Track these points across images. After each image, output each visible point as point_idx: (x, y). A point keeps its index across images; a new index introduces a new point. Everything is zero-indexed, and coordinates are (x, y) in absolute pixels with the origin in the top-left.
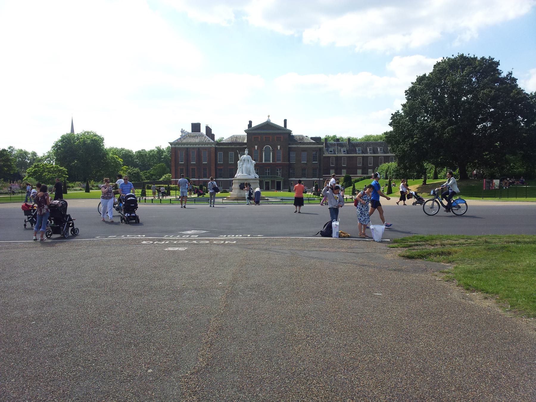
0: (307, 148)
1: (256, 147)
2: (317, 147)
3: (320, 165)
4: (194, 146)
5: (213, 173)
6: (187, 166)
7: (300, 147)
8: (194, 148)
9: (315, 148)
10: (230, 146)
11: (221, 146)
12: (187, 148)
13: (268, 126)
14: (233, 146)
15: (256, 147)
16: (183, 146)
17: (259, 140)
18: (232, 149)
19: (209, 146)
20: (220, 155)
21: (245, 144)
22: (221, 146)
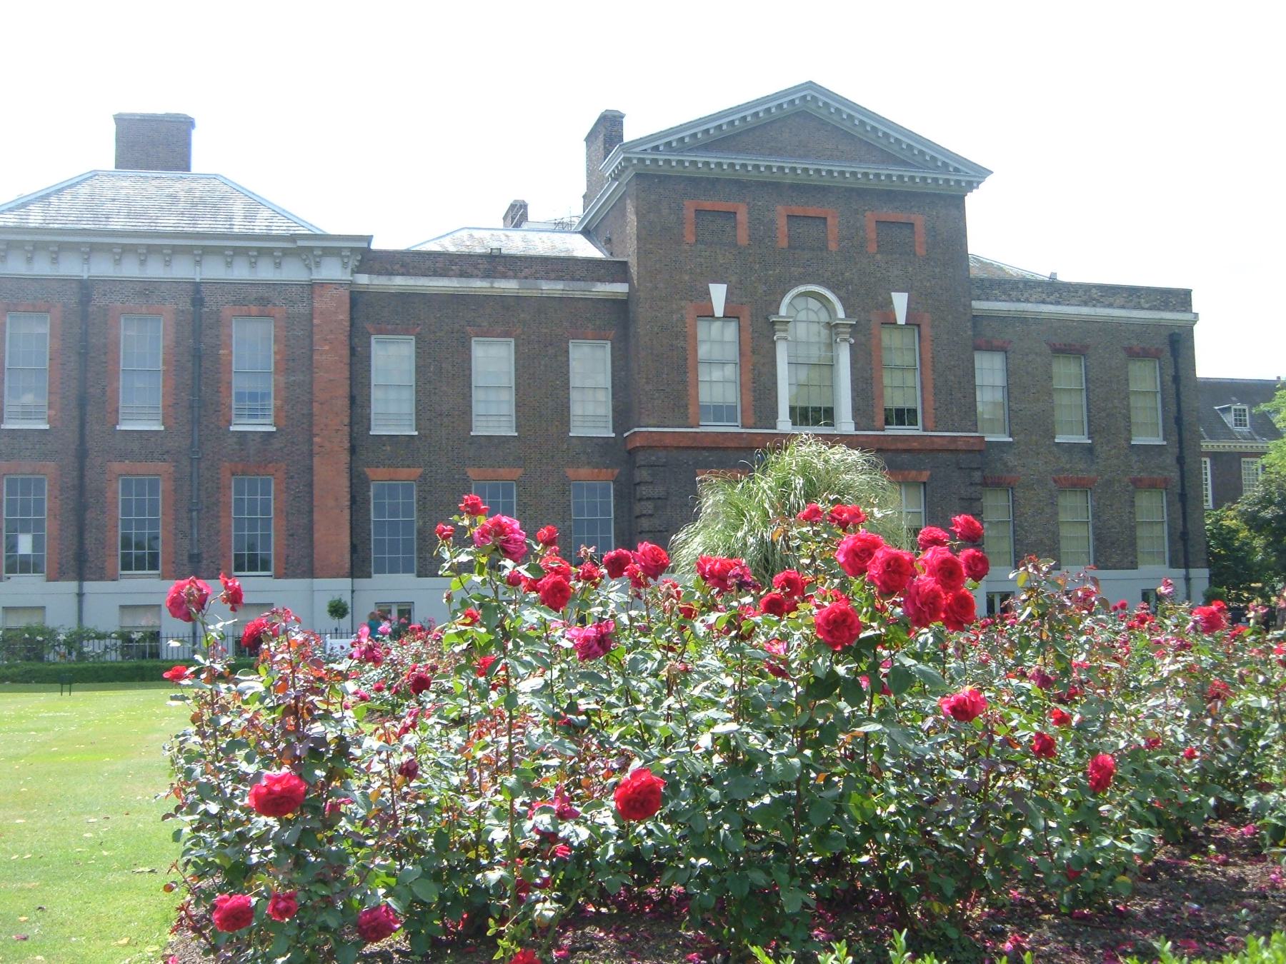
0: (1087, 323)
1: (718, 293)
2: (1158, 325)
3: (1180, 460)
4: (155, 270)
5: (333, 535)
6: (82, 454)
7: (1037, 320)
8: (147, 289)
9: (1146, 326)
10: (479, 285)
11: (400, 282)
12: (86, 288)
13: (808, 117)
14: (508, 286)
15: (718, 293)
16: (42, 267)
17: (743, 236)
18: (499, 316)
19: (293, 272)
20: (393, 361)
21: (616, 270)
22: (400, 282)
